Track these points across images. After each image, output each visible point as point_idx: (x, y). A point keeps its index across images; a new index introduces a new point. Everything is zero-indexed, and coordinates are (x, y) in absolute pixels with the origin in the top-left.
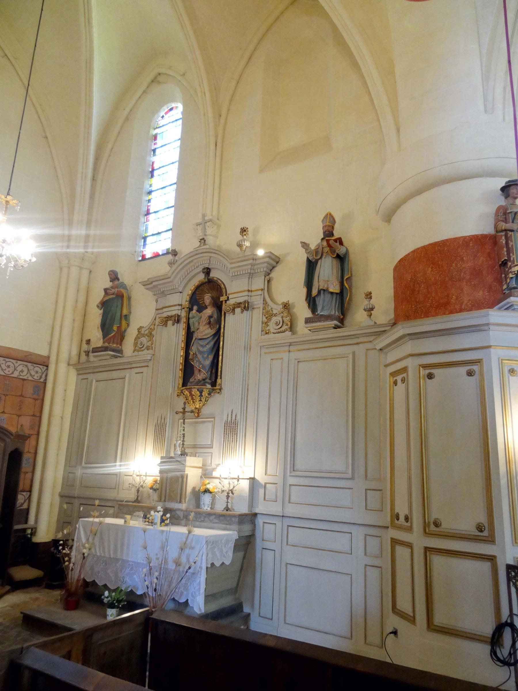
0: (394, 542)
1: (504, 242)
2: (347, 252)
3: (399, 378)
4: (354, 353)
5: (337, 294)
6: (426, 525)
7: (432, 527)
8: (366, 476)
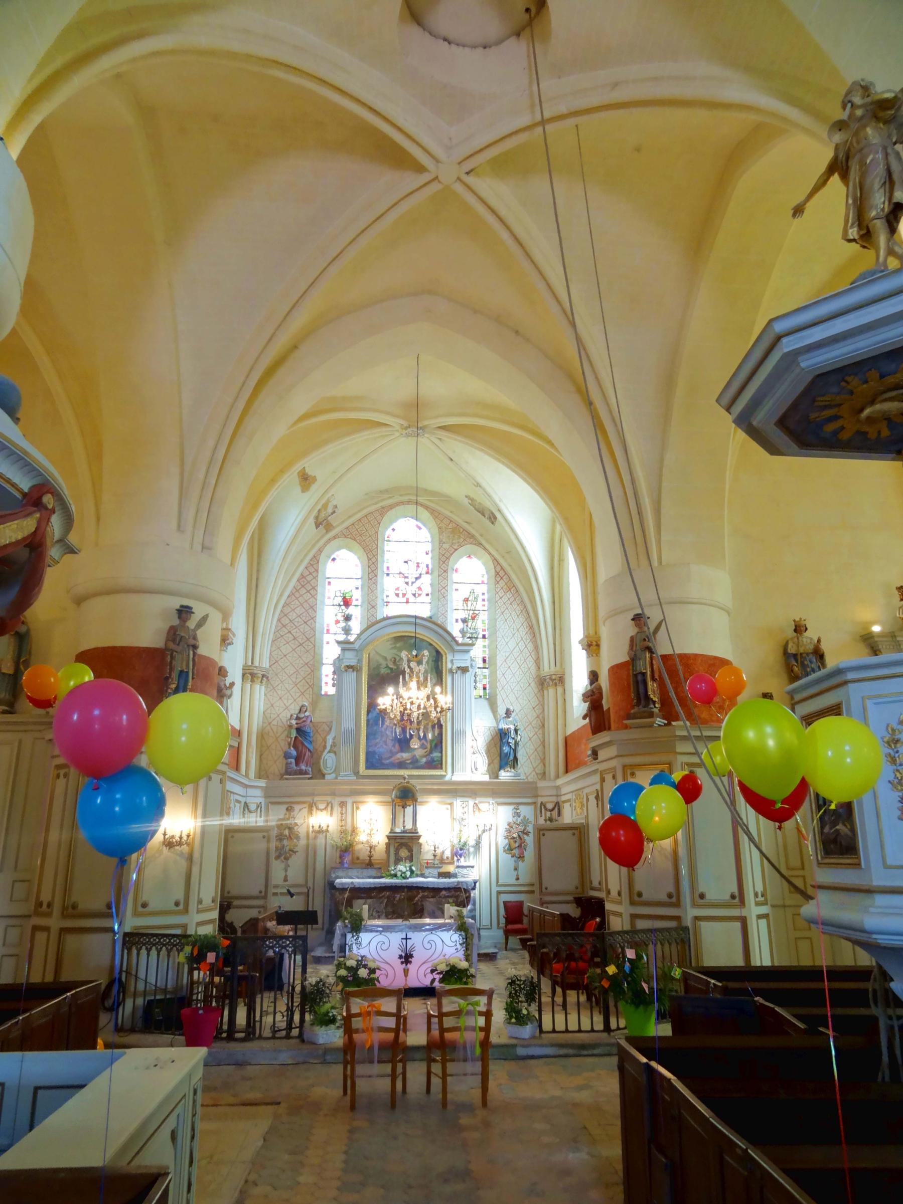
0: (35, 928)
2: (28, 631)
3: (62, 772)
4: (20, 742)
5: (10, 675)
6: (64, 908)
7: (71, 910)
8: (16, 867)
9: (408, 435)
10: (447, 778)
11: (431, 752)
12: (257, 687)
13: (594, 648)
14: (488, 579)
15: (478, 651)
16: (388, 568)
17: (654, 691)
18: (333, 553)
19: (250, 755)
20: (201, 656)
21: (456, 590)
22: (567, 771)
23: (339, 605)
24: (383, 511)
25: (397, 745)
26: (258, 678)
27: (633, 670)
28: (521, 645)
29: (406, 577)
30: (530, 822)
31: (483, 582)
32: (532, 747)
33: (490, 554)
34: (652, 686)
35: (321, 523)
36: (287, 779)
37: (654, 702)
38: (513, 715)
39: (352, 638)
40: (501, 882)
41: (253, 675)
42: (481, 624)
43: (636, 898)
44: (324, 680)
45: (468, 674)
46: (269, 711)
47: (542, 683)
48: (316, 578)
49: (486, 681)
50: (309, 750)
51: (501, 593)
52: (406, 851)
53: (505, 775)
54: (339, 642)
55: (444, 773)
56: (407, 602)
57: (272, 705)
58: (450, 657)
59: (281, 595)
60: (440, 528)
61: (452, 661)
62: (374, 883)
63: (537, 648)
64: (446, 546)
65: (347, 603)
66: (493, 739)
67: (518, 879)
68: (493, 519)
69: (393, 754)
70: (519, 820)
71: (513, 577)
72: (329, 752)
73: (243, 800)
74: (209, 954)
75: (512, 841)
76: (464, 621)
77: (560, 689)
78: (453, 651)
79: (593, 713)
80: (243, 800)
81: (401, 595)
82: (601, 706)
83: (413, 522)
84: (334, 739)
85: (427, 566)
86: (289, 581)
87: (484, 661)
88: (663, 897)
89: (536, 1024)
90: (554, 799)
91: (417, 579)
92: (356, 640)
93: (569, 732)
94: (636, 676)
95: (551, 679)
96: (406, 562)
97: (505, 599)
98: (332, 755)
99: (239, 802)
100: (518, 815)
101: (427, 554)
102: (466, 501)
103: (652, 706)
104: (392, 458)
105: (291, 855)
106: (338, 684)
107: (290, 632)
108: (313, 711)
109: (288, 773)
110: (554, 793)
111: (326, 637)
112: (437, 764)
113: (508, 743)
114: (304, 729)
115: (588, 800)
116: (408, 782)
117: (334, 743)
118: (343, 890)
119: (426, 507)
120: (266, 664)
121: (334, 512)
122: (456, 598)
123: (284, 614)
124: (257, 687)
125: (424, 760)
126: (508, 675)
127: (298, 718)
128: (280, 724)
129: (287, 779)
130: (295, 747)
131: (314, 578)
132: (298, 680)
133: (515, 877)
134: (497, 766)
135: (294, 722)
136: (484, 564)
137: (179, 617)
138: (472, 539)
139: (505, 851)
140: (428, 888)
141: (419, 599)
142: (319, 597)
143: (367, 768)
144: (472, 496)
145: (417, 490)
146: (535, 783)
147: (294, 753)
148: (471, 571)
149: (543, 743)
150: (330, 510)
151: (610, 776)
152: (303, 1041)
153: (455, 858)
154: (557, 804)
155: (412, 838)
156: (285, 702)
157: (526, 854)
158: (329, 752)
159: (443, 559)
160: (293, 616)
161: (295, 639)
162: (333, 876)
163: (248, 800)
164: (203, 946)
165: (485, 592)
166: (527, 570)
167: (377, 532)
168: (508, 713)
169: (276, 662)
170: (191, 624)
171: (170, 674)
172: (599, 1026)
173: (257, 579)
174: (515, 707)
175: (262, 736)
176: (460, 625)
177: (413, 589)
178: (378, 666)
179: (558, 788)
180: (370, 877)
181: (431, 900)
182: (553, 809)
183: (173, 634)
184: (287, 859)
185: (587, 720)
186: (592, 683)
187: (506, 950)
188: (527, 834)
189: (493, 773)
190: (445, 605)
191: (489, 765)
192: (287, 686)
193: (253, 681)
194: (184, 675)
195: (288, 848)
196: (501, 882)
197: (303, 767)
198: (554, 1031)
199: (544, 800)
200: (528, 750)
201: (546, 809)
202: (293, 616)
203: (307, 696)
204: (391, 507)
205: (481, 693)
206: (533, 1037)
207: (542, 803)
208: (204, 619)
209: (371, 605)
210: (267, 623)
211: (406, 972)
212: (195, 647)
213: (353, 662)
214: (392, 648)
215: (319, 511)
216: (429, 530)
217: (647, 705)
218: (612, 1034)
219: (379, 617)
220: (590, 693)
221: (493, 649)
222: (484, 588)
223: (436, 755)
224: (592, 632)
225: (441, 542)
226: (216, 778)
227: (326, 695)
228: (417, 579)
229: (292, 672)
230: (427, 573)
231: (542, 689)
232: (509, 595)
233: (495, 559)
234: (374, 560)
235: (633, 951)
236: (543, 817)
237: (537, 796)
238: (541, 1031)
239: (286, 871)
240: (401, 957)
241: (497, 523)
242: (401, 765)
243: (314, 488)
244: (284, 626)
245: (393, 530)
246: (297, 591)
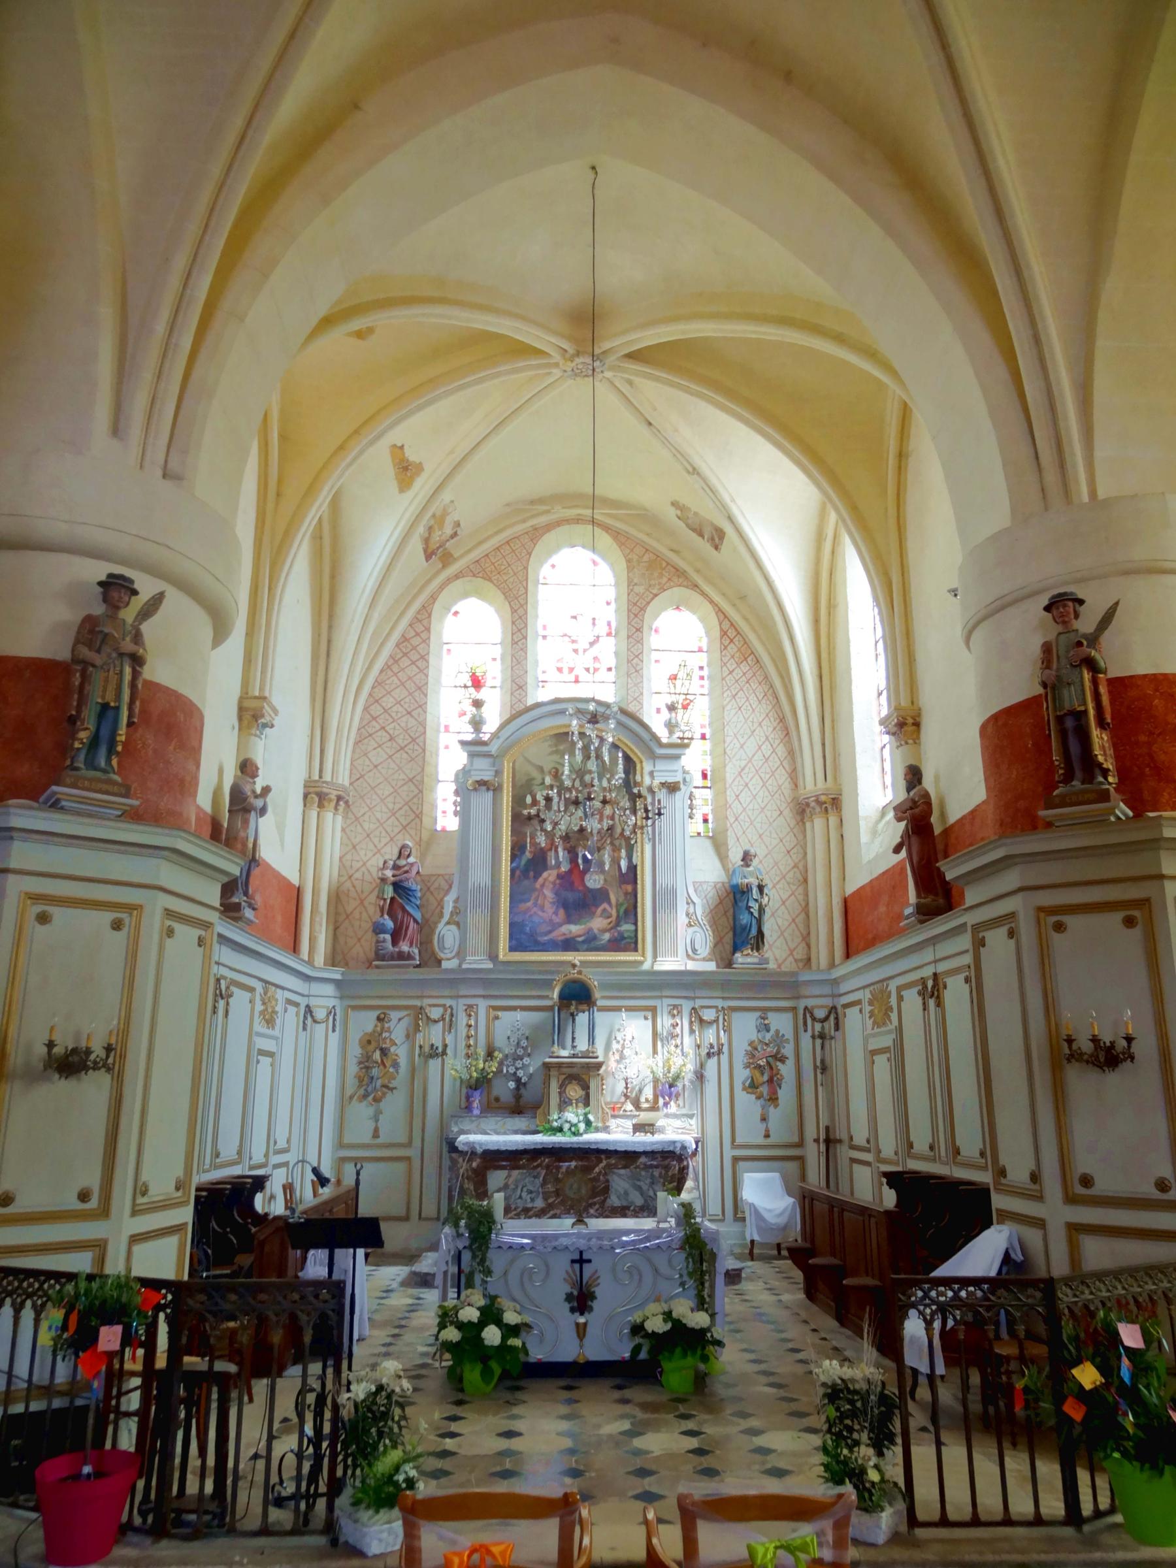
1: (77, 683)
9: (576, 374)
10: (646, 966)
11: (618, 924)
12: (329, 816)
13: (910, 728)
14: (710, 643)
15: (695, 760)
16: (545, 628)
17: (1103, 748)
18: (455, 603)
19: (317, 928)
20: (149, 684)
21: (657, 661)
22: (848, 956)
23: (465, 687)
24: (536, 534)
25: (561, 912)
26: (330, 800)
27: (1055, 710)
28: (767, 749)
29: (573, 642)
30: (787, 1041)
31: (700, 650)
32: (787, 916)
33: (711, 602)
34: (1100, 740)
35: (433, 553)
36: (377, 967)
37: (1105, 773)
38: (755, 862)
39: (486, 738)
40: (739, 1141)
41: (322, 798)
42: (697, 718)
43: (1080, 1190)
44: (441, 806)
45: (678, 795)
46: (348, 857)
47: (802, 810)
48: (426, 641)
49: (707, 809)
50: (415, 921)
51: (732, 665)
52: (578, 1088)
53: (745, 959)
54: (463, 743)
55: (640, 958)
56: (577, 681)
57: (354, 847)
58: (647, 767)
59: (369, 669)
60: (629, 561)
61: (651, 774)
62: (524, 1143)
63: (792, 754)
64: (639, 589)
65: (477, 683)
66: (721, 902)
67: (767, 1136)
68: (717, 538)
69: (555, 926)
70: (768, 1037)
71: (752, 637)
72: (448, 923)
73: (303, 1002)
74: (104, 1331)
75: (757, 1074)
76: (672, 708)
77: (833, 820)
78: (653, 757)
79: (915, 840)
80: (303, 1002)
81: (566, 670)
82: (929, 827)
83: (589, 554)
84: (456, 901)
85: (609, 624)
86: (382, 644)
87: (705, 776)
88: (1148, 1190)
89: (901, 1505)
90: (828, 1002)
91: (592, 644)
92: (491, 740)
93: (850, 889)
94: (1060, 720)
95: (820, 803)
96: (575, 617)
97: (738, 673)
98: (453, 928)
99: (297, 1005)
101: (608, 603)
102: (672, 513)
103: (1101, 779)
104: (551, 425)
105: (384, 1094)
106: (464, 813)
107: (383, 728)
108: (423, 856)
109: (379, 956)
110: (827, 990)
111: (444, 738)
112: (630, 943)
113: (748, 908)
114: (405, 884)
115: (900, 998)
116: (580, 973)
117: (455, 907)
118: (471, 1153)
119: (606, 528)
120: (344, 779)
121: (455, 534)
122: (656, 675)
123: (373, 700)
124: (329, 816)
125: (607, 936)
126: (745, 797)
127: (396, 867)
128: (368, 878)
129: (377, 967)
130: (391, 914)
131: (424, 641)
132: (397, 806)
133: (763, 1133)
134: (729, 948)
135: (389, 873)
136: (702, 620)
137: (105, 600)
138: (680, 576)
140: (616, 1152)
141: (599, 676)
142: (431, 672)
143: (512, 949)
144: (685, 500)
145: (594, 500)
146: (793, 974)
147: (390, 924)
148: (681, 633)
149: (806, 909)
150: (448, 531)
151: (1003, 931)
152: (334, 1542)
153: (661, 1101)
154: (834, 1008)
155: (588, 1067)
156: (376, 840)
158: (448, 923)
159: (635, 610)
160: (388, 702)
161: (392, 739)
162: (455, 1129)
163: (313, 1002)
164: (92, 1307)
165: (704, 664)
166: (775, 623)
167: (526, 568)
168: (747, 858)
169: (362, 776)
170: (128, 614)
171: (79, 709)
172: (1054, 1506)
173: (329, 641)
174: (759, 850)
175: (337, 898)
176: (665, 715)
177: (586, 660)
178: (530, 782)
179: (836, 982)
180: (516, 1132)
181: (622, 1172)
182: (827, 1018)
183: (91, 632)
184: (377, 1100)
185: (903, 853)
186: (909, 790)
187: (752, 1260)
188: (783, 1060)
189: (722, 959)
190: (639, 685)
191: (715, 945)
192: (378, 815)
193: (321, 805)
194: (110, 714)
195: (379, 1083)
196: (739, 1141)
197: (404, 947)
198: (944, 1521)
199: (810, 1003)
200: (780, 921)
201: (814, 1019)
202: (388, 702)
203: (413, 832)
204: (549, 527)
205: (700, 827)
206: (896, 1538)
207: (806, 1008)
208: (157, 601)
209: (517, 682)
210: (346, 714)
211: (581, 1331)
212: (137, 661)
213: (487, 776)
214: (551, 753)
215: (430, 529)
216: (612, 566)
217: (1089, 778)
218: (1086, 1528)
219: (530, 702)
220: (910, 804)
221: (720, 754)
222: (703, 659)
223: (627, 927)
224: (905, 703)
225: (630, 582)
226: (186, 934)
227: (444, 830)
228: (592, 644)
229: (387, 793)
230: (609, 634)
231: (802, 821)
232: (744, 667)
233: (720, 611)
234: (521, 612)
235: (1136, 1328)
236: (810, 1032)
237: (798, 998)
238: (913, 1521)
239: (377, 1121)
240: (569, 1298)
241: (724, 548)
242: (568, 945)
243: (419, 482)
244: (374, 719)
245: (553, 566)
246: (396, 662)
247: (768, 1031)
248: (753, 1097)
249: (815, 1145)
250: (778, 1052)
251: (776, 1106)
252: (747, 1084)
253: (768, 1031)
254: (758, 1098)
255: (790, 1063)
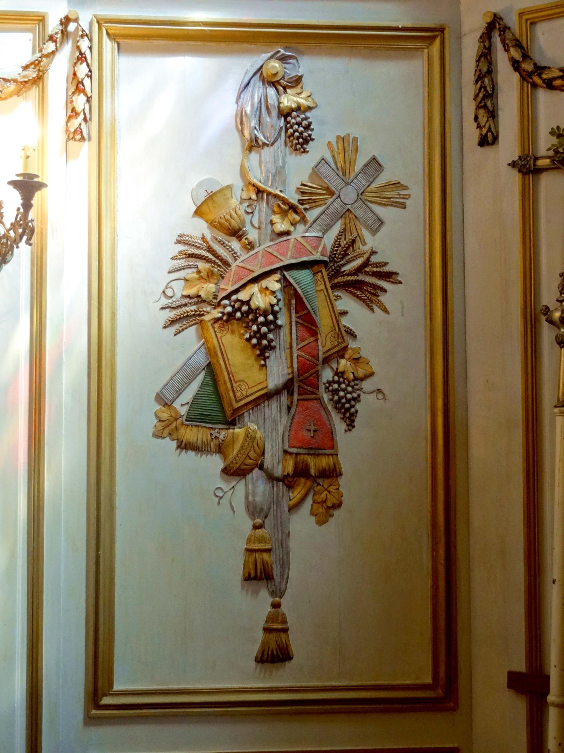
67: (275, 654)
75: (234, 347)
100: (297, 131)
139: (167, 428)
157: (351, 447)
188: (365, 281)
207: (495, 25)
236: (509, 146)
247: (300, 140)
248: (216, 463)
249: (517, 708)
250: (345, 248)
251: (326, 510)
252: (181, 406)
253: (300, 140)
254: (235, 472)
255: (405, 302)
